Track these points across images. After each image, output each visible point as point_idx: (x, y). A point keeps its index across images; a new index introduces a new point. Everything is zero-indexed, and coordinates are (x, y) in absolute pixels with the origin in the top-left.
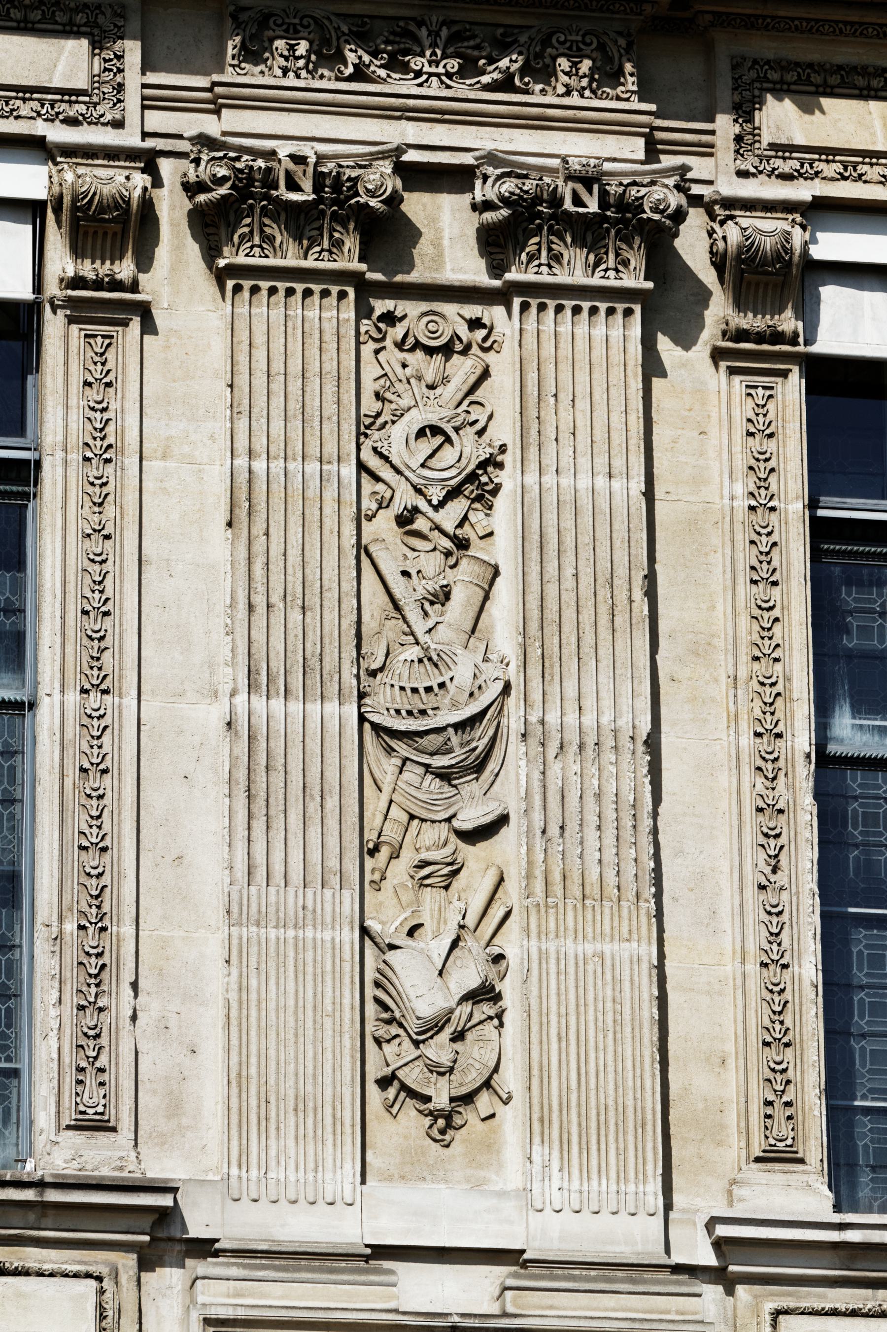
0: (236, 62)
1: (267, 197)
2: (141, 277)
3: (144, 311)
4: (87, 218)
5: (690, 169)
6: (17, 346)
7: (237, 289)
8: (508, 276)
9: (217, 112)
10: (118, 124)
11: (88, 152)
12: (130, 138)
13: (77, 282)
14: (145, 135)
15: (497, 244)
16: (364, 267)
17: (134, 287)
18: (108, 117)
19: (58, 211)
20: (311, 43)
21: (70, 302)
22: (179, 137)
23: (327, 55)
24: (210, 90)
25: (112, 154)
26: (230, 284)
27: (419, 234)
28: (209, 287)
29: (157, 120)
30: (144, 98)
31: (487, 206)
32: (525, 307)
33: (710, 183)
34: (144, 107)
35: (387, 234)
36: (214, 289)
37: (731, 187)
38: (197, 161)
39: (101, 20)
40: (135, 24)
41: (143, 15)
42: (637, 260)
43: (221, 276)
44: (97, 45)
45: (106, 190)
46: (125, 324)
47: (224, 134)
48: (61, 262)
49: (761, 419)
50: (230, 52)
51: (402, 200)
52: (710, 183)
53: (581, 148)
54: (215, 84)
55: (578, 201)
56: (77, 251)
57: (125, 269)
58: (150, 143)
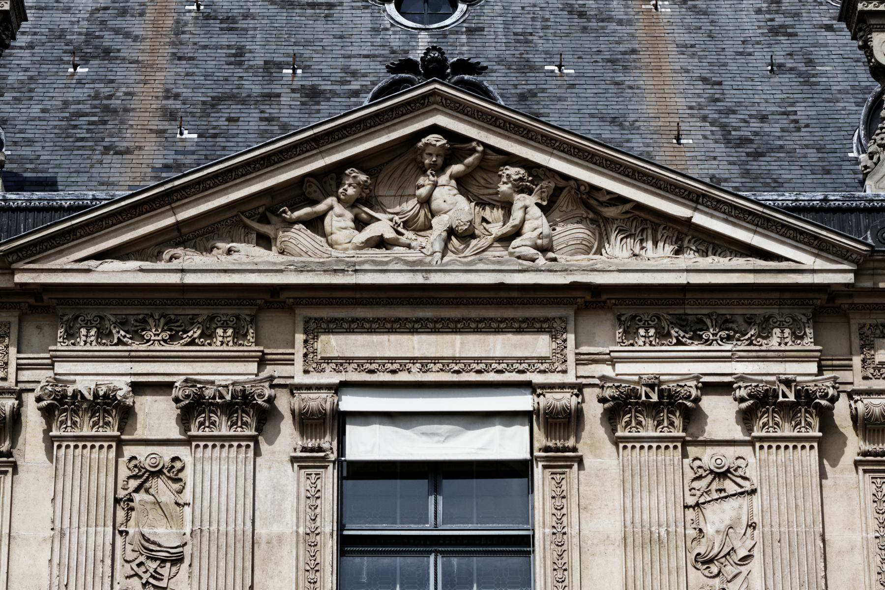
0: (620, 340)
1: (775, 404)
2: (578, 446)
3: (580, 461)
4: (551, 418)
5: (838, 378)
6: (524, 481)
7: (625, 447)
8: (753, 434)
9: (613, 365)
10: (564, 372)
11: (552, 387)
12: (570, 378)
13: (547, 449)
14: (577, 377)
15: (746, 418)
16: (684, 434)
17: (574, 449)
18: (559, 369)
19: (538, 417)
20: (656, 329)
21: (547, 459)
22: (594, 377)
23: (663, 335)
24: (609, 354)
25: (562, 386)
26: (621, 445)
27: (706, 416)
28: (610, 448)
29: (584, 370)
30: (577, 360)
31: (742, 400)
32: (761, 447)
33: (852, 383)
34: (577, 364)
35: (692, 416)
36: (614, 448)
37: (861, 384)
38: (602, 387)
39: (555, 325)
40: (571, 326)
41: (576, 320)
42: (815, 422)
43: (616, 441)
44: (554, 337)
45: (558, 404)
46: (570, 467)
47: (617, 375)
48: (541, 440)
49: (879, 493)
50: (618, 335)
51: (700, 400)
52: (852, 383)
53: (791, 369)
54: (611, 351)
55: (647, 396)
56: (548, 435)
57: (571, 443)
58: (579, 381)
